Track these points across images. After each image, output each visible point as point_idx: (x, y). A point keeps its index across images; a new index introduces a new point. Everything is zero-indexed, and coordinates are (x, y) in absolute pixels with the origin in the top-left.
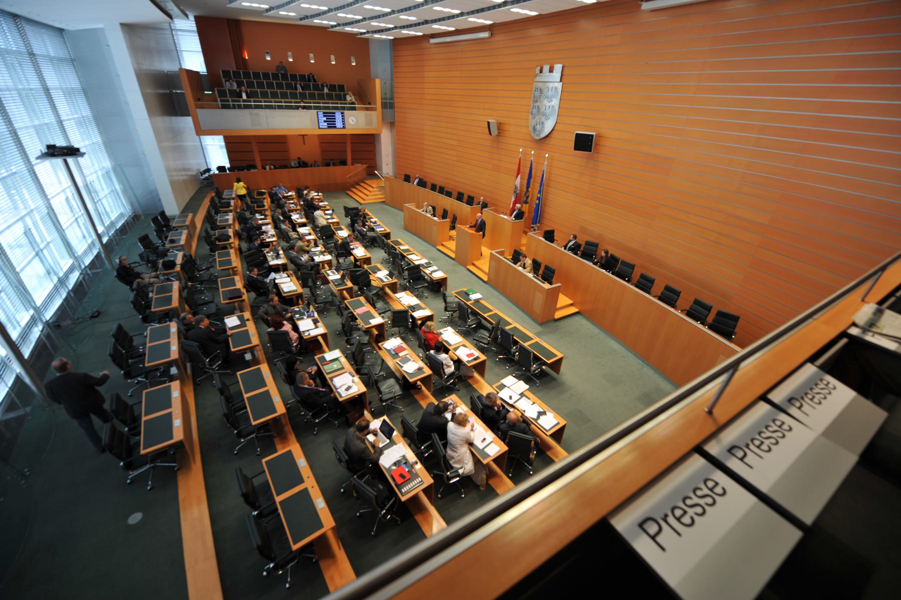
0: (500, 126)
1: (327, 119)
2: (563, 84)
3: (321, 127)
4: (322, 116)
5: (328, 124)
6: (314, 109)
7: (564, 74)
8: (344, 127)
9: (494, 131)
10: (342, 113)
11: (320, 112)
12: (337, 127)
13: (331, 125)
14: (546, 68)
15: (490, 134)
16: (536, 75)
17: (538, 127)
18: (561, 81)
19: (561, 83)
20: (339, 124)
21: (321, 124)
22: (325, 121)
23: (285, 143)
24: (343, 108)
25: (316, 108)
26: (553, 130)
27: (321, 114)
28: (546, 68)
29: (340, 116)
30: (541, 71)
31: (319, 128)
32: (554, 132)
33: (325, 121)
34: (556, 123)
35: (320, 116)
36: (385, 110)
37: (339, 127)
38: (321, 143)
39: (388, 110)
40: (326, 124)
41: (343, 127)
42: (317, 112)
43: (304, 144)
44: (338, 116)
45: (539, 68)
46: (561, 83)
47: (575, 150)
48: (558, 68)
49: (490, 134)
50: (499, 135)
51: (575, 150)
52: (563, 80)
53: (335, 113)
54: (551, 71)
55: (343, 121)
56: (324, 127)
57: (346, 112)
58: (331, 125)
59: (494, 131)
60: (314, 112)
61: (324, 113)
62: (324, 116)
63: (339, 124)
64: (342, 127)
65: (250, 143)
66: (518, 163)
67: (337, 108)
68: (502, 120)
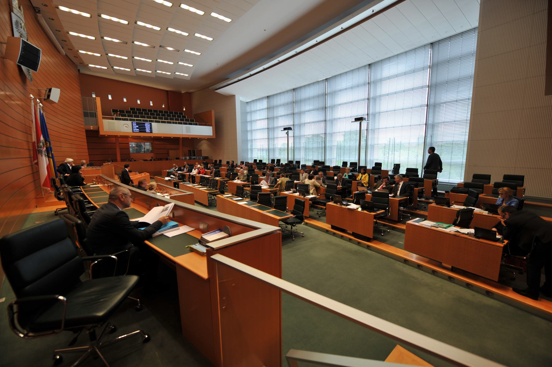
1: (139, 126)
3: (134, 131)
4: (136, 124)
5: (139, 130)
6: (130, 121)
8: (151, 132)
10: (150, 124)
11: (134, 122)
12: (147, 132)
13: (142, 129)
20: (148, 130)
21: (134, 130)
22: (137, 128)
24: (152, 121)
25: (130, 120)
27: (135, 124)
29: (149, 125)
31: (133, 132)
33: (137, 128)
35: (133, 125)
37: (148, 132)
40: (138, 130)
41: (151, 132)
42: (132, 122)
44: (147, 125)
53: (145, 124)
55: (150, 129)
56: (136, 131)
57: (153, 123)
58: (142, 129)
60: (129, 123)
61: (137, 123)
62: (137, 125)
63: (148, 130)
64: (150, 132)
67: (147, 121)
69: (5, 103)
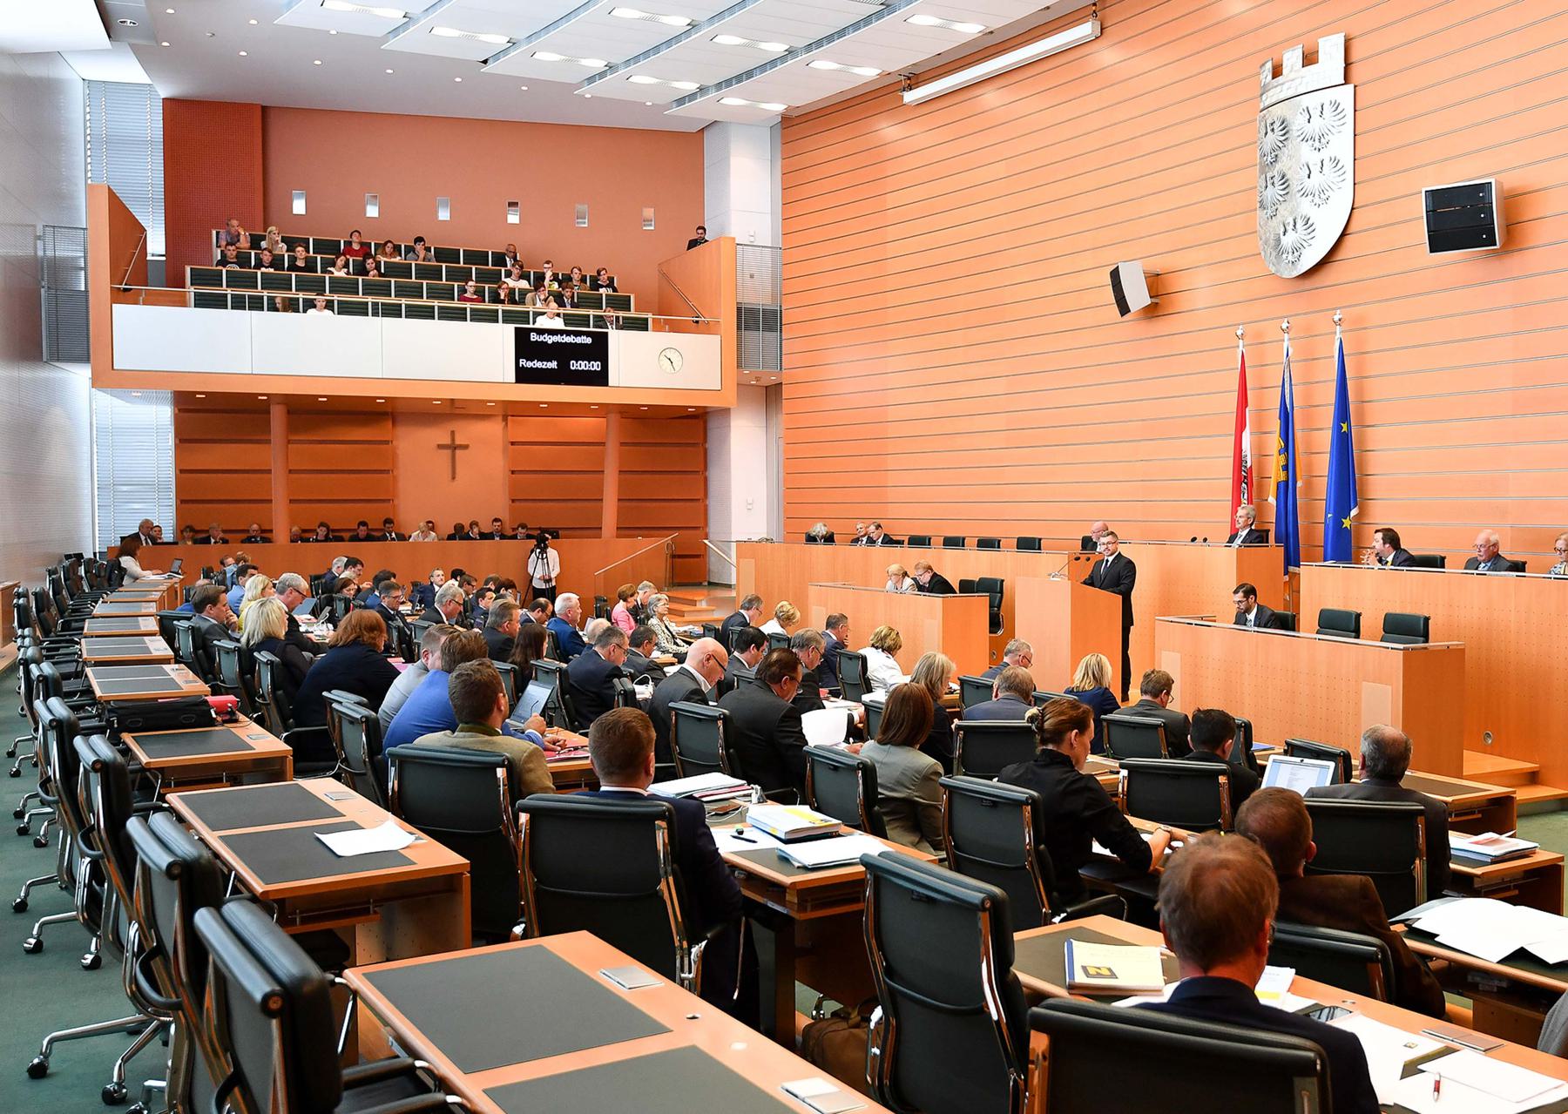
0: (1155, 283)
2: (1355, 87)
7: (1354, 57)
9: (1138, 297)
14: (1292, 58)
15: (1124, 308)
16: (1265, 89)
17: (1288, 241)
18: (1347, 80)
19: (1350, 87)
23: (387, 472)
26: (1344, 234)
28: (1292, 58)
30: (1277, 72)
32: (1348, 239)
34: (1353, 209)
36: (749, 335)
38: (513, 472)
39: (757, 338)
43: (454, 478)
45: (1269, 66)
46: (1350, 87)
47: (1431, 252)
48: (1331, 50)
49: (1124, 308)
50: (1153, 311)
51: (1431, 252)
52: (1356, 70)
54: (1309, 59)
59: (1138, 297)
65: (269, 471)
66: (1235, 386)
68: (1157, 265)
69: (1339, 308)
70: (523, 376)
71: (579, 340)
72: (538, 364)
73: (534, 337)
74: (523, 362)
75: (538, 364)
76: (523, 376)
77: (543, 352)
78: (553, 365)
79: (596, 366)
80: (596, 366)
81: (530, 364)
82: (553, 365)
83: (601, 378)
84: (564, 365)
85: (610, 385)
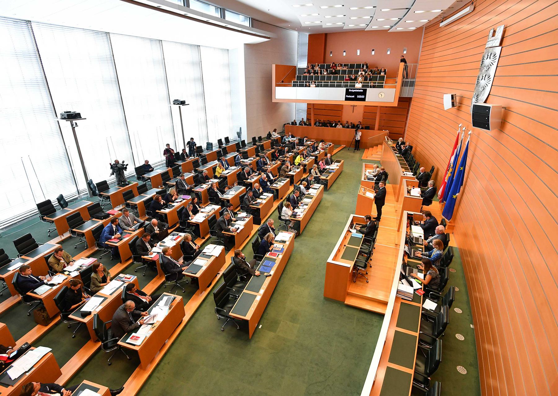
43: (353, 112)
70: (347, 99)
71: (360, 91)
72: (350, 97)
73: (350, 90)
74: (347, 96)
75: (350, 97)
76: (347, 99)
77: (351, 94)
78: (353, 97)
79: (363, 97)
80: (363, 97)
81: (348, 97)
82: (353, 97)
83: (364, 100)
84: (356, 97)
85: (366, 101)
